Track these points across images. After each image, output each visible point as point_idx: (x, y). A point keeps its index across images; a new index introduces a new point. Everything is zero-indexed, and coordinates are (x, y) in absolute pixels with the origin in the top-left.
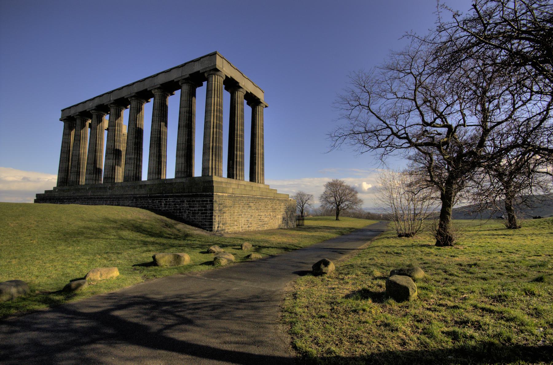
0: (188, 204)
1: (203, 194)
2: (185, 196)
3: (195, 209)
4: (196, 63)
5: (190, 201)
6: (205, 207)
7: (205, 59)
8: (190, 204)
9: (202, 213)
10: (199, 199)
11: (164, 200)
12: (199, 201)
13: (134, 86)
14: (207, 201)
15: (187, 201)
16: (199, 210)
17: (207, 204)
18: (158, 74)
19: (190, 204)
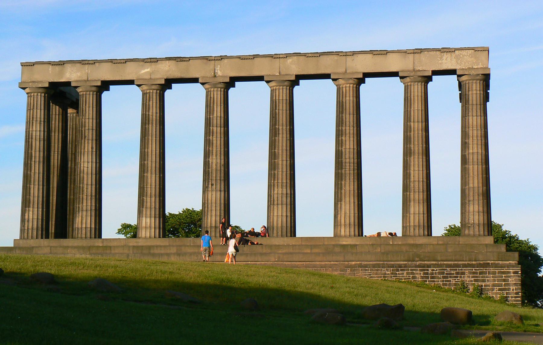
0: (473, 277)
1: (499, 264)
2: (465, 266)
3: (488, 283)
4: (445, 56)
5: (474, 273)
6: (504, 280)
7: (464, 52)
8: (477, 277)
9: (500, 290)
10: (492, 270)
11: (421, 270)
12: (494, 273)
13: (289, 60)
14: (509, 273)
15: (470, 273)
16: (494, 285)
17: (510, 277)
18: (354, 53)
19: (477, 277)
